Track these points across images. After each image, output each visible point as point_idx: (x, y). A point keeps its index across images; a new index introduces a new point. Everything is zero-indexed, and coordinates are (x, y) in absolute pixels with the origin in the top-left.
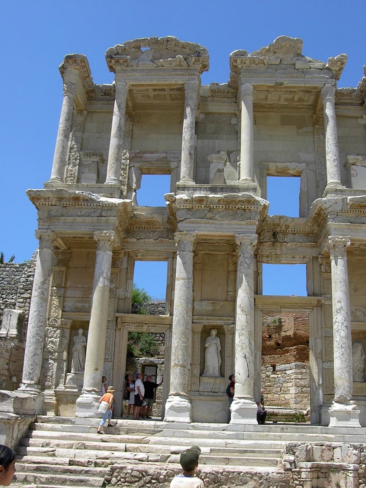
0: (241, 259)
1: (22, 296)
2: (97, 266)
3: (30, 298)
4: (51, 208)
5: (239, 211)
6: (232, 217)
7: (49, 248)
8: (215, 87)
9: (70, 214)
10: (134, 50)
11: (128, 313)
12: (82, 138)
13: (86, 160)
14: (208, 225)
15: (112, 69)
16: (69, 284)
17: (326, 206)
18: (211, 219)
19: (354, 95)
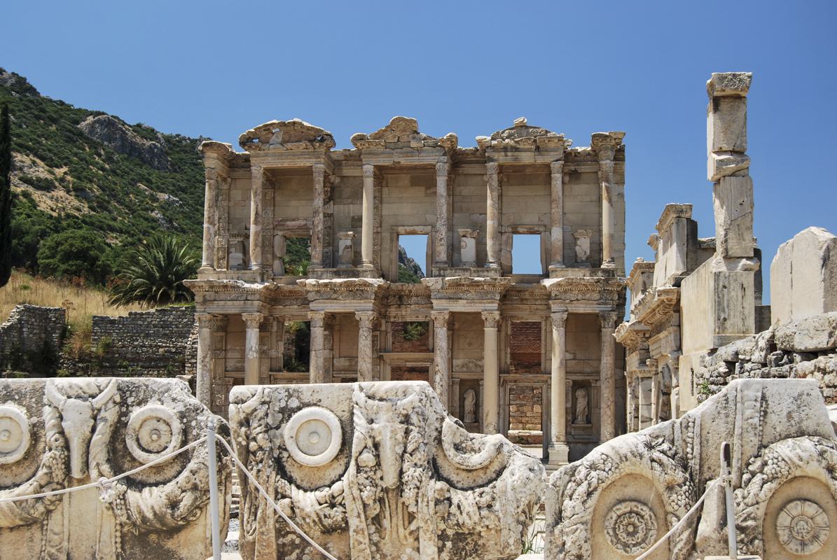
0: (361, 332)
1: (190, 361)
2: (247, 341)
3: (196, 363)
4: (205, 293)
5: (358, 292)
6: (352, 298)
7: (207, 327)
8: (348, 153)
9: (221, 298)
10: (265, 133)
11: (280, 371)
12: (229, 207)
13: (232, 239)
14: (333, 305)
15: (246, 150)
16: (229, 347)
17: (429, 284)
18: (335, 299)
19: (478, 153)
